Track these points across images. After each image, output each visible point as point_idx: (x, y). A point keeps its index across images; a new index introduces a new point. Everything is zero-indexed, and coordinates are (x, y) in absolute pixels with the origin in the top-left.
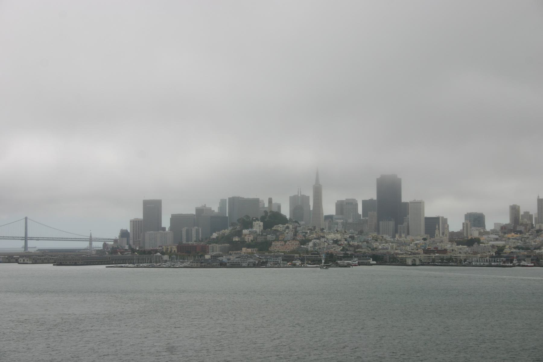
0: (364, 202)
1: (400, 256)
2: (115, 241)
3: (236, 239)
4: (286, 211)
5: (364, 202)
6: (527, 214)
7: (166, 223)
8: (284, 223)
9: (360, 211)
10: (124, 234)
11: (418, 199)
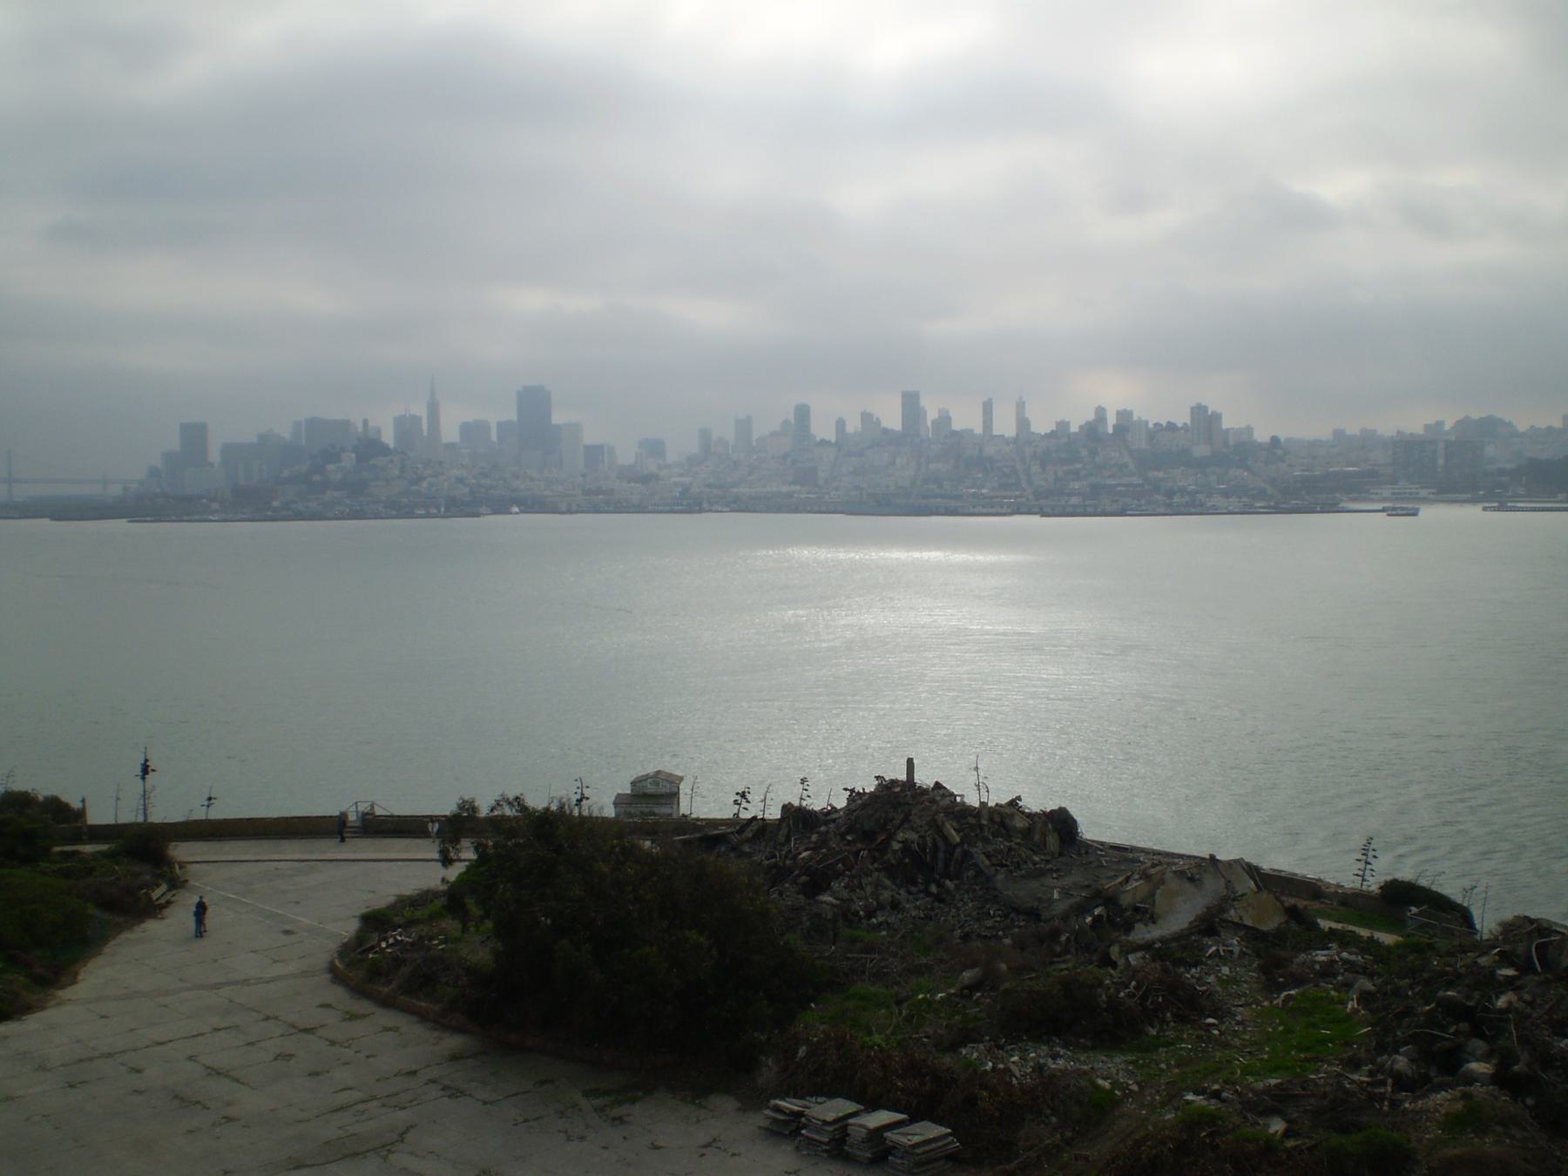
0: (499, 425)
1: (549, 499)
3: (317, 478)
4: (388, 438)
5: (499, 425)
7: (215, 456)
9: (494, 437)
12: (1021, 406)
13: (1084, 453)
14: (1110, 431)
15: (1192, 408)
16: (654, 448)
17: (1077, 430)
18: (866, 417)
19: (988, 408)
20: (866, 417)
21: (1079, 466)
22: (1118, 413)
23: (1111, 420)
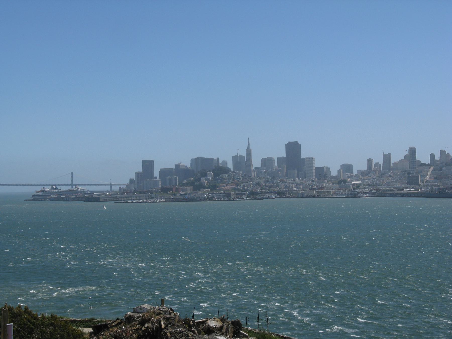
0: (279, 159)
2: (127, 186)
3: (197, 183)
4: (230, 166)
5: (279, 159)
7: (157, 174)
8: (227, 173)
9: (276, 164)
10: (131, 181)
11: (311, 157)
16: (347, 168)
18: (442, 153)
20: (442, 153)
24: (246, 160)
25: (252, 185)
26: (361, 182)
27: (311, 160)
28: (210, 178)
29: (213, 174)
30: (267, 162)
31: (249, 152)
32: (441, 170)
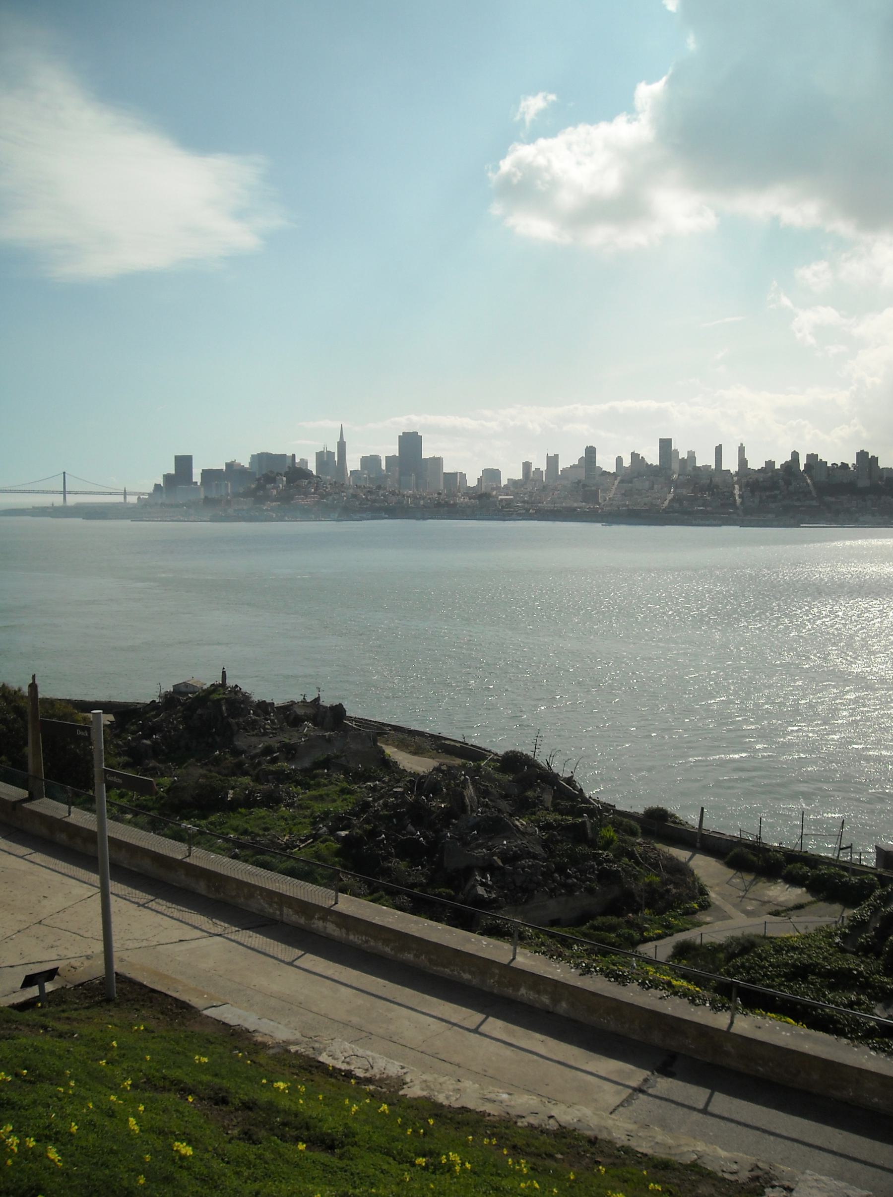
2: (149, 494)
4: (312, 467)
6: (538, 469)
7: (197, 477)
9: (384, 467)
11: (437, 456)
12: (742, 450)
13: (781, 483)
14: (802, 468)
15: (858, 454)
16: (492, 475)
17: (779, 467)
18: (634, 456)
19: (719, 450)
20: (634, 456)
21: (777, 492)
22: (808, 456)
23: (803, 461)
24: (336, 459)
25: (345, 498)
26: (512, 497)
27: (437, 462)
28: (281, 485)
29: (285, 479)
30: (370, 462)
31: (342, 445)
32: (631, 482)
